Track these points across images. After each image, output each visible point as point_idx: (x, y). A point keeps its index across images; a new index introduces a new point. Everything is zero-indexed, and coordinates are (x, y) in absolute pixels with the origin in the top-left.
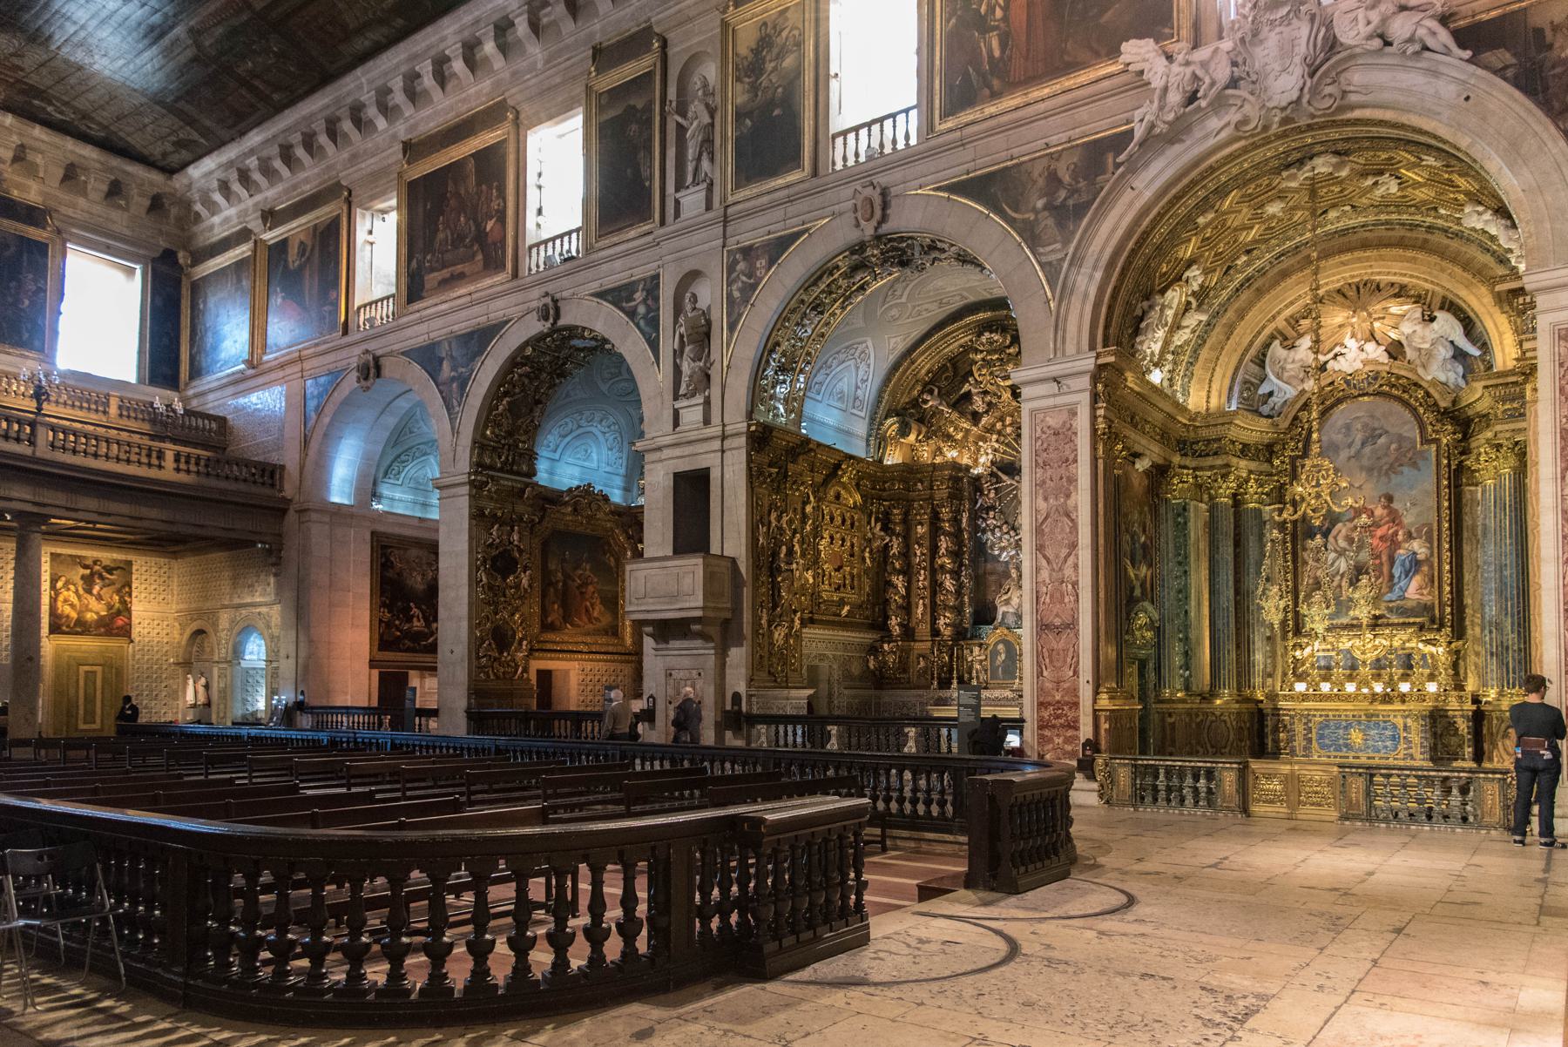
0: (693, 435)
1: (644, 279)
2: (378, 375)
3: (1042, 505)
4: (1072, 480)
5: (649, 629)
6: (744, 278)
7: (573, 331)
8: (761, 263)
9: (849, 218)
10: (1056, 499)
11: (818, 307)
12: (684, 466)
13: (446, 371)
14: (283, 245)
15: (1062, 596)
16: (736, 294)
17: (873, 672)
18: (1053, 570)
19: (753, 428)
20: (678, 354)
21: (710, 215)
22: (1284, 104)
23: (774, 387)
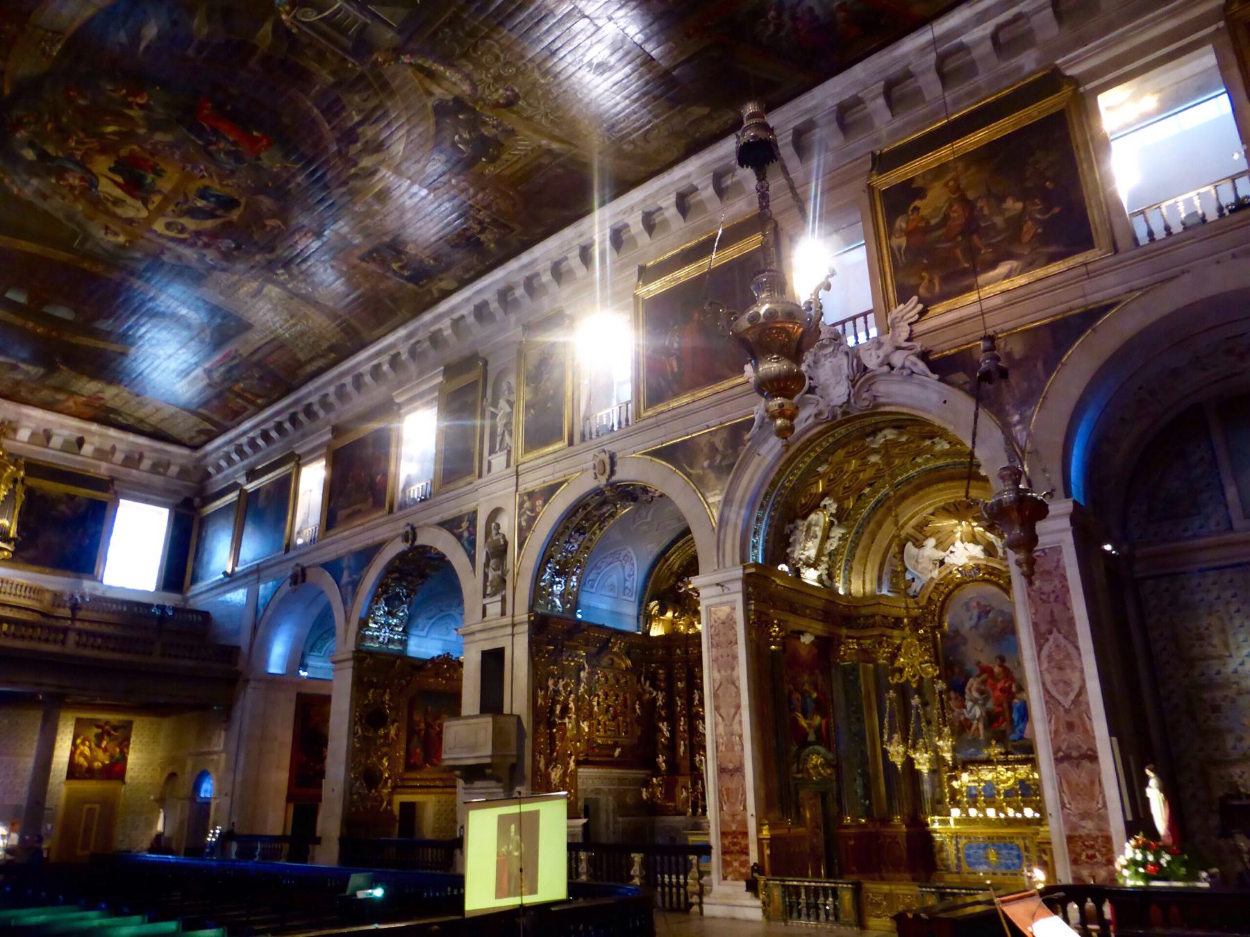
0: (494, 624)
1: (468, 514)
2: (304, 580)
4: (735, 657)
5: (458, 773)
6: (528, 513)
7: (425, 549)
8: (539, 503)
9: (591, 472)
10: (725, 671)
11: (580, 530)
13: (345, 578)
14: (257, 492)
16: (524, 524)
17: (645, 802)
19: (532, 618)
20: (487, 565)
21: (508, 471)
22: (840, 404)
23: (551, 586)
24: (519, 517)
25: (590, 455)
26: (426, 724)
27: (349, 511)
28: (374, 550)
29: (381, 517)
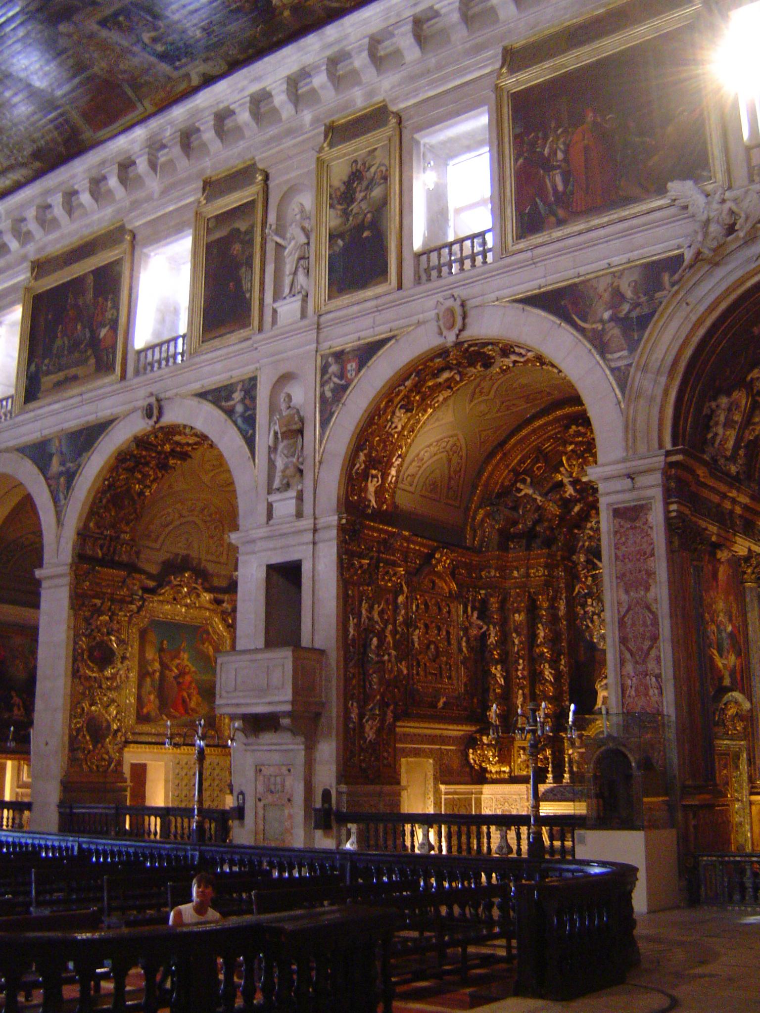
0: (286, 528)
1: (243, 381)
3: (624, 597)
6: (336, 380)
12: (277, 558)
13: (55, 466)
15: (647, 688)
16: (329, 394)
18: (637, 662)
19: (344, 521)
20: (273, 450)
21: (305, 322)
24: (322, 385)
25: (431, 302)
26: (162, 664)
27: (61, 376)
28: (99, 429)
29: (111, 385)
